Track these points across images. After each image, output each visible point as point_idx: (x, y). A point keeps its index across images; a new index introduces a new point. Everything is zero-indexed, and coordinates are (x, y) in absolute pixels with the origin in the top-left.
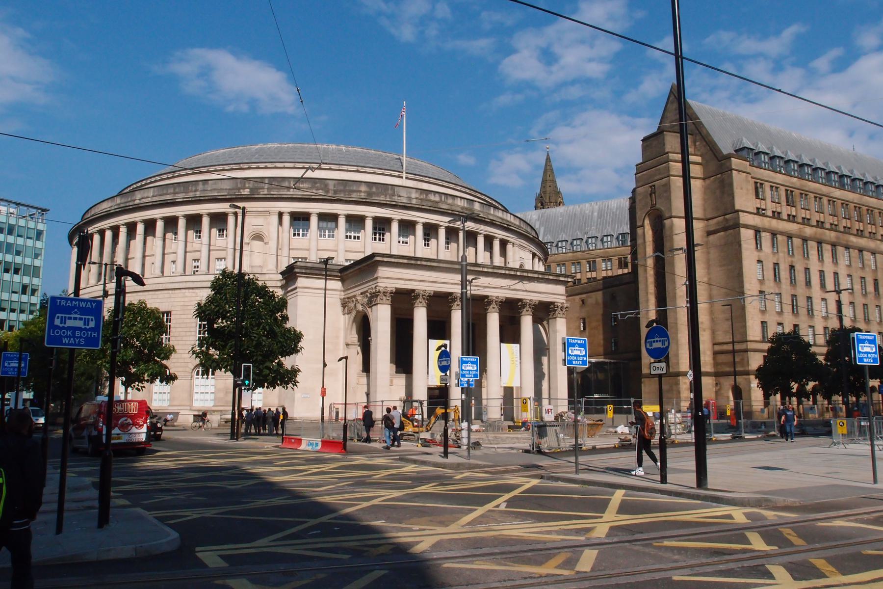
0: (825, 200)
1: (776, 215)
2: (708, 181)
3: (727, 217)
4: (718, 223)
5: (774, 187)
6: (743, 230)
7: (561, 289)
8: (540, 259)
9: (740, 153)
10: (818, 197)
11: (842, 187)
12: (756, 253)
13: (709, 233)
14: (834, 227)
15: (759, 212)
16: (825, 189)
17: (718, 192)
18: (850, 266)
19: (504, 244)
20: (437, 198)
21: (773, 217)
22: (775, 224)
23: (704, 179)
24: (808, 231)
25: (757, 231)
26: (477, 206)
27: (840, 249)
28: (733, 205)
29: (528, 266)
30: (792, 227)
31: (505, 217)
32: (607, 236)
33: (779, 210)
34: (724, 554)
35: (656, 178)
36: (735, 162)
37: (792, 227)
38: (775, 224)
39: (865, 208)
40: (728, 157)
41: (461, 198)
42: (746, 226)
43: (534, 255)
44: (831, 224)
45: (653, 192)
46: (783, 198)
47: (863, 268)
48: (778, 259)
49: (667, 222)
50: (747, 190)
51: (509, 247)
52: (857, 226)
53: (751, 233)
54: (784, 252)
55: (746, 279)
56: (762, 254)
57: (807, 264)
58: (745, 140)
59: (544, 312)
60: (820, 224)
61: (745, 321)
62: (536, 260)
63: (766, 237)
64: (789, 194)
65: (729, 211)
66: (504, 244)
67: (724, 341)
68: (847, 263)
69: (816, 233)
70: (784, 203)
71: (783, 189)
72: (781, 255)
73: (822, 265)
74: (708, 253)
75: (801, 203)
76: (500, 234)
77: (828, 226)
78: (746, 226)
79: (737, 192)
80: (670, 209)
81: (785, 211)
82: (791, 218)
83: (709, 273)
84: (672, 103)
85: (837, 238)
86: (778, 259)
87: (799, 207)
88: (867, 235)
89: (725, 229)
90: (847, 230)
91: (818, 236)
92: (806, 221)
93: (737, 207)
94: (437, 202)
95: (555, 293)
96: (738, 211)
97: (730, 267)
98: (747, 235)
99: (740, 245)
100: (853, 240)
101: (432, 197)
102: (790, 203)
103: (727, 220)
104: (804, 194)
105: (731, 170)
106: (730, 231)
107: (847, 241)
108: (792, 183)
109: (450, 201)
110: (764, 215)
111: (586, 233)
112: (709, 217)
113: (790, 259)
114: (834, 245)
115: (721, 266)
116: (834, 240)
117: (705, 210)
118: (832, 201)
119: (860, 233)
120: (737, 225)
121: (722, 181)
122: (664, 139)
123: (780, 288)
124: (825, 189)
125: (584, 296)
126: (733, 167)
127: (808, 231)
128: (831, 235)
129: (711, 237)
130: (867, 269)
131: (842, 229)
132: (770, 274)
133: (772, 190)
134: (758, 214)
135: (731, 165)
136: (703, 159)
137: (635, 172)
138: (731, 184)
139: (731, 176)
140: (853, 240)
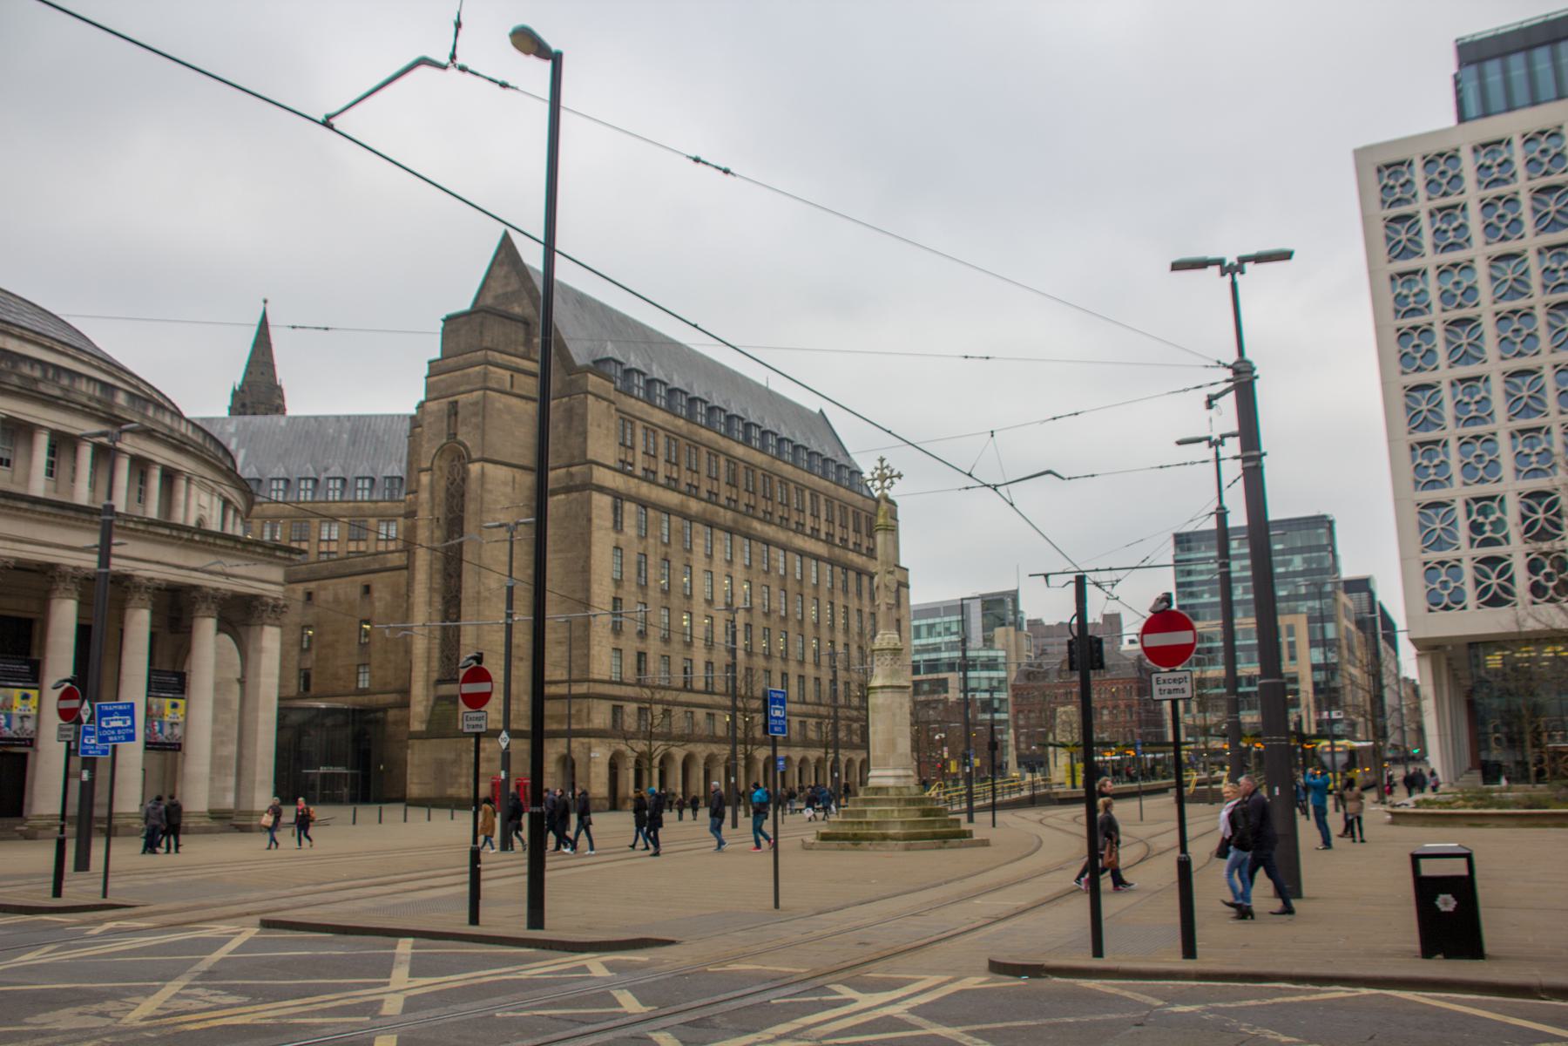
1: (649, 476)
3: (574, 469)
5: (651, 429)
6: (596, 496)
7: (277, 573)
8: (236, 510)
9: (602, 367)
10: (714, 452)
11: (747, 442)
12: (613, 535)
14: (732, 504)
15: (624, 468)
16: (723, 443)
18: (749, 567)
19: (169, 476)
20: (37, 373)
22: (645, 490)
24: (694, 506)
25: (619, 497)
26: (121, 399)
28: (584, 453)
29: (214, 525)
30: (672, 498)
31: (176, 425)
32: (363, 478)
33: (653, 468)
34: (584, 1023)
35: (462, 389)
37: (672, 498)
40: (586, 370)
41: (90, 379)
42: (601, 489)
43: (226, 503)
45: (453, 410)
47: (767, 572)
48: (646, 548)
49: (475, 468)
51: (181, 484)
55: (594, 577)
56: (622, 538)
58: (610, 346)
59: (240, 615)
60: (712, 497)
61: (588, 647)
62: (231, 513)
66: (169, 476)
69: (705, 510)
72: (651, 541)
76: (161, 455)
77: (723, 501)
78: (601, 489)
79: (593, 431)
82: (671, 484)
84: (501, 264)
85: (735, 521)
88: (777, 520)
93: (590, 456)
94: (36, 381)
95: (263, 579)
98: (602, 503)
99: (590, 520)
101: (26, 369)
103: (571, 475)
104: (695, 444)
105: (587, 392)
106: (575, 495)
107: (749, 527)
109: (65, 381)
110: (631, 475)
111: (326, 470)
116: (730, 523)
119: (767, 519)
120: (588, 486)
123: (645, 595)
124: (723, 443)
125: (312, 586)
127: (694, 506)
132: (631, 571)
134: (622, 471)
137: (426, 372)
138: (584, 418)
139: (584, 404)
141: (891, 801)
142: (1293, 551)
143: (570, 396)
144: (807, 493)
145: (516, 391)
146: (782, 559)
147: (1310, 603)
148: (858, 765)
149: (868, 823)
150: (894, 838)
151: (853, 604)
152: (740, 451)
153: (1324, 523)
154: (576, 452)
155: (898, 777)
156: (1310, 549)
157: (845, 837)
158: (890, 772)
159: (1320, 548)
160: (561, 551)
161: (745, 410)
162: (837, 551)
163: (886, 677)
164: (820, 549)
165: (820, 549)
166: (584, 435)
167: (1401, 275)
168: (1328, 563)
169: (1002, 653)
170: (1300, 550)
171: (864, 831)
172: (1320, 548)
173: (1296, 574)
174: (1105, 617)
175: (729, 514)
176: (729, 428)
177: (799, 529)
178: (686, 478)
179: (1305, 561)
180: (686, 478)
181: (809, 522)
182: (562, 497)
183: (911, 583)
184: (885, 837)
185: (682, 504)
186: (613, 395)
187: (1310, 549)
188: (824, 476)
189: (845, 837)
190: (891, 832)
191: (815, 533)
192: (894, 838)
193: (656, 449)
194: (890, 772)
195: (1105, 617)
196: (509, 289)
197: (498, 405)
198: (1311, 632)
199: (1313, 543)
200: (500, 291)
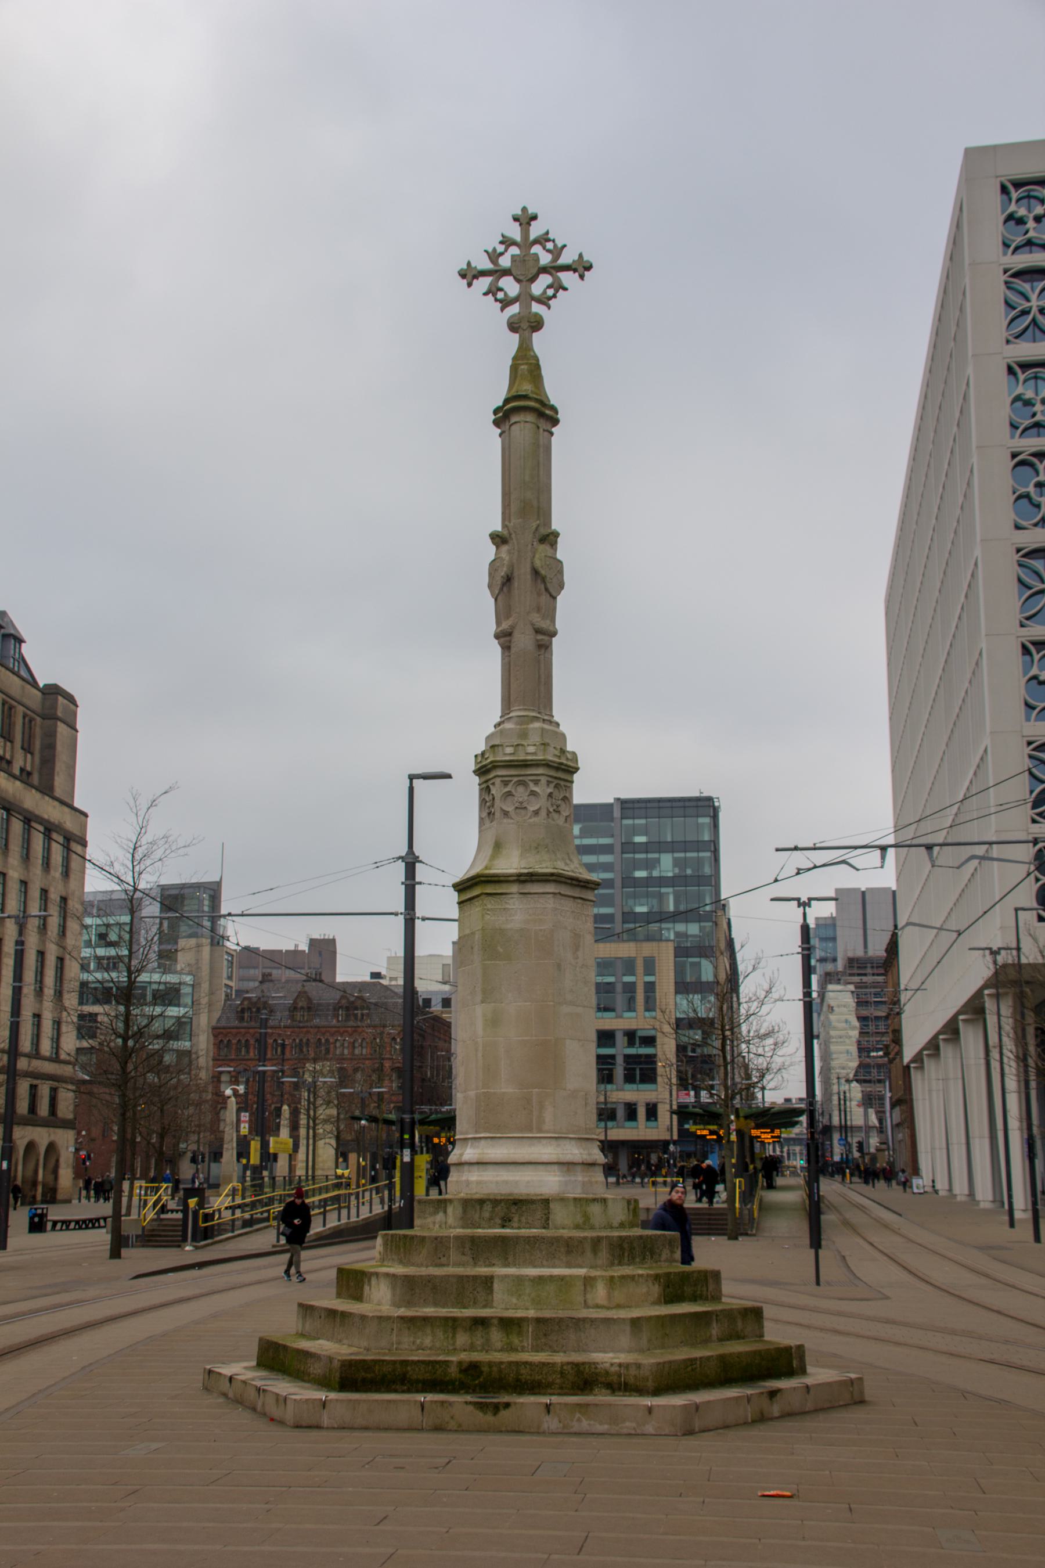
141: (569, 1249)
142: (659, 846)
147: (680, 927)
148: (42, 1150)
149: (508, 1324)
150: (620, 1384)
153: (705, 807)
155: (567, 1166)
156: (685, 846)
157: (434, 1380)
158: (547, 1151)
159: (698, 846)
163: (531, 847)
167: (1025, 366)
168: (707, 870)
169: (188, 979)
170: (671, 847)
171: (494, 1353)
172: (698, 846)
173: (662, 882)
174: (313, 943)
179: (676, 863)
183: (89, 838)
184: (584, 1380)
187: (685, 846)
189: (434, 1380)
190: (607, 1357)
192: (620, 1384)
194: (547, 1151)
195: (313, 943)
198: (679, 970)
199: (691, 837)
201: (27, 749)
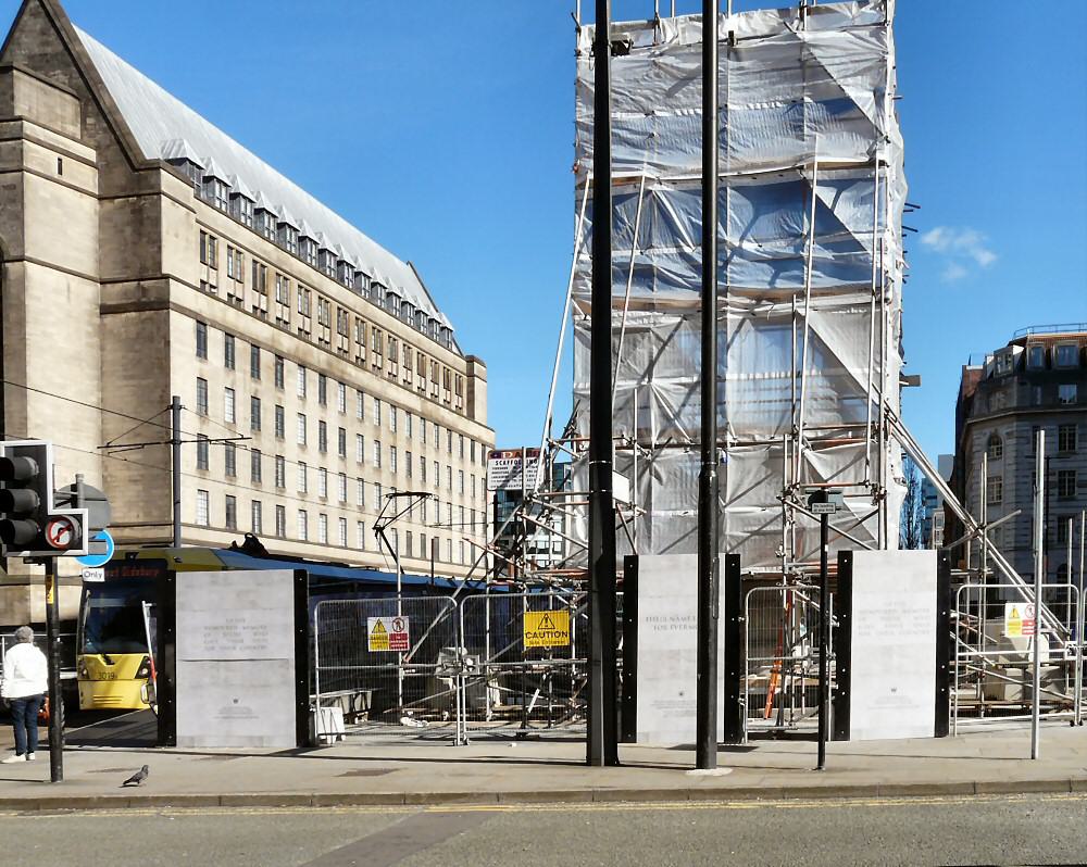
0: (314, 295)
1: (235, 302)
2: (108, 205)
4: (125, 293)
5: (235, 250)
10: (305, 288)
11: (340, 280)
13: (105, 310)
15: (205, 288)
17: (128, 230)
21: (228, 303)
22: (232, 317)
23: (100, 198)
27: (332, 384)
28: (159, 264)
36: (167, 181)
38: (232, 317)
39: (370, 324)
40: (154, 167)
42: (183, 310)
44: (320, 339)
46: (249, 275)
48: (233, 383)
50: (187, 240)
52: (356, 350)
53: (190, 324)
54: (245, 372)
56: (204, 366)
57: (280, 399)
60: (303, 334)
63: (215, 338)
64: (259, 268)
65: (150, 274)
67: (127, 521)
68: (341, 408)
69: (297, 348)
70: (249, 284)
71: (249, 257)
73: (304, 405)
74: (102, 349)
75: (274, 289)
78: (183, 310)
80: (21, 243)
81: (251, 299)
82: (259, 314)
83: (102, 389)
85: (329, 364)
86: (233, 383)
87: (273, 298)
89: (139, 307)
90: (343, 354)
91: (300, 355)
92: (282, 325)
93: (165, 271)
96: (167, 277)
97: (144, 382)
99: (168, 343)
100: (352, 372)
102: (261, 287)
103: (144, 290)
104: (284, 276)
105: (159, 193)
107: (343, 372)
108: (265, 252)
112: (106, 277)
113: (253, 385)
114: (323, 375)
115: (125, 378)
116: (323, 366)
117: (100, 262)
118: (324, 299)
119: (360, 363)
120: (163, 304)
121: (137, 211)
122: (11, 86)
126: (163, 189)
128: (320, 358)
129: (109, 319)
130: (367, 423)
131: (335, 351)
133: (230, 255)
134: (201, 290)
135: (159, 185)
136: (99, 155)
138: (157, 222)
140: (352, 372)
143: (139, 196)
144: (401, 343)
145: (64, 178)
146: (375, 408)
151: (444, 461)
152: (332, 288)
154: (149, 264)
160: (132, 377)
161: (338, 249)
162: (430, 405)
164: (414, 402)
165: (414, 402)
166: (157, 242)
175: (324, 356)
176: (322, 263)
177: (392, 377)
178: (276, 311)
180: (276, 311)
181: (402, 375)
182: (133, 314)
185: (273, 340)
186: (193, 203)
188: (417, 328)
191: (407, 385)
193: (242, 273)
196: (49, 50)
197: (42, 193)
200: (37, 51)
201: (459, 394)
